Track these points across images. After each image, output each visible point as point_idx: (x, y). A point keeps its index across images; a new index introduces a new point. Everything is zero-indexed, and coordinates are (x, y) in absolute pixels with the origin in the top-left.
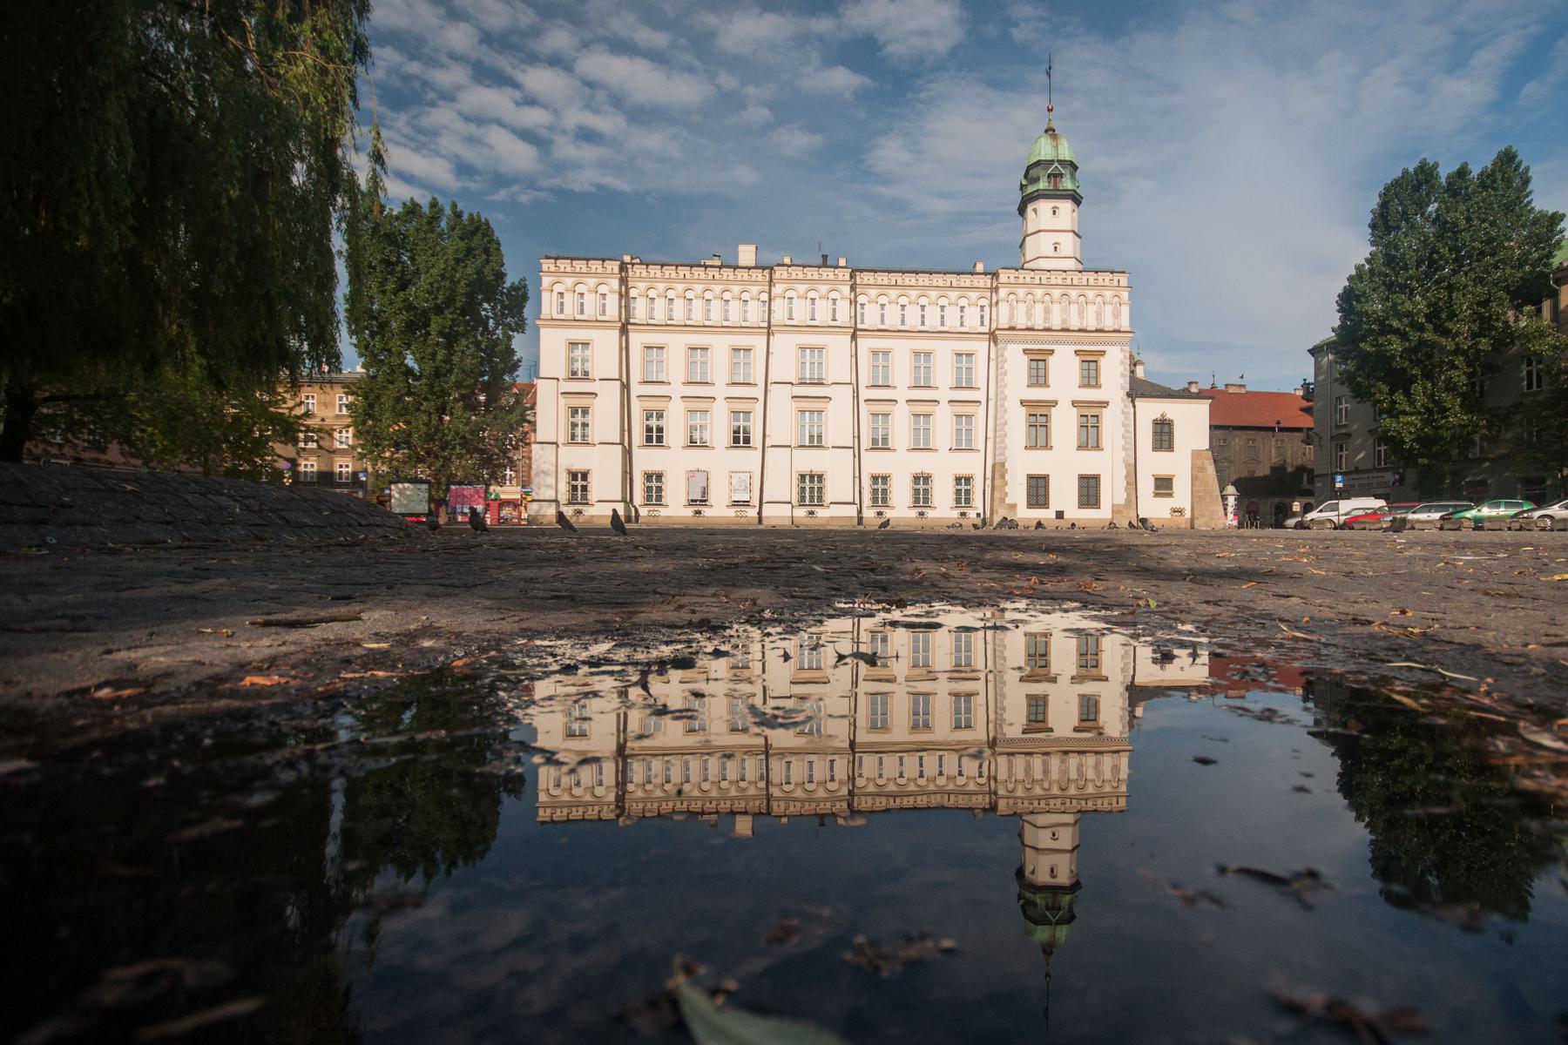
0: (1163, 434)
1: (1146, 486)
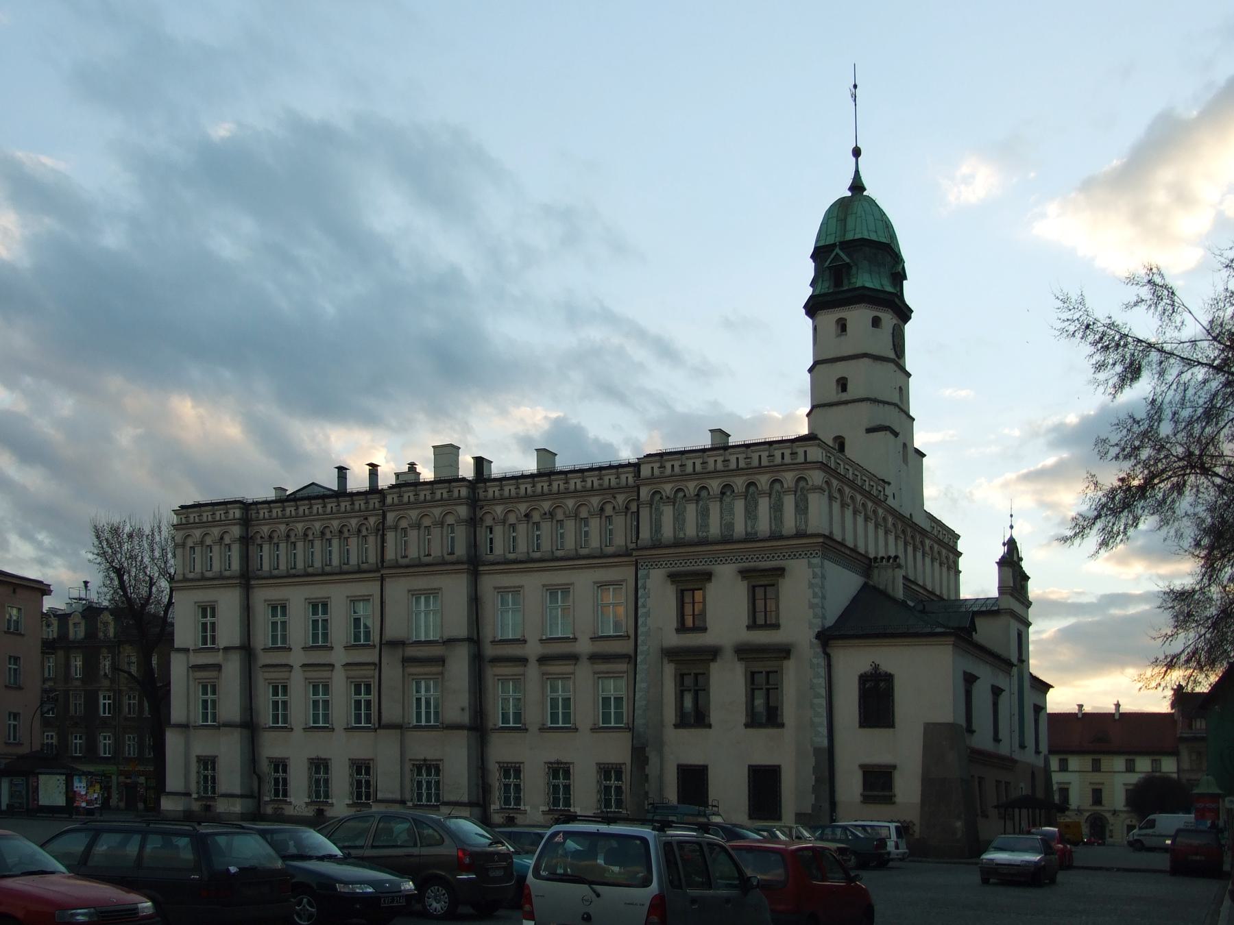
0: (877, 700)
1: (850, 786)
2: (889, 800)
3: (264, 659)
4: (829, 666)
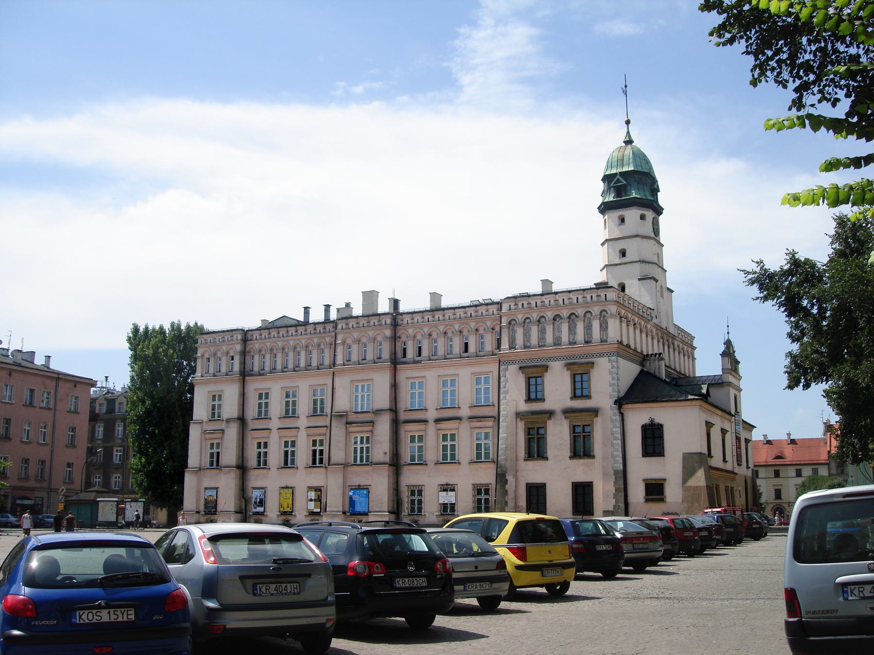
0: (653, 440)
1: (637, 493)
2: (662, 500)
3: (251, 425)
4: (623, 420)
